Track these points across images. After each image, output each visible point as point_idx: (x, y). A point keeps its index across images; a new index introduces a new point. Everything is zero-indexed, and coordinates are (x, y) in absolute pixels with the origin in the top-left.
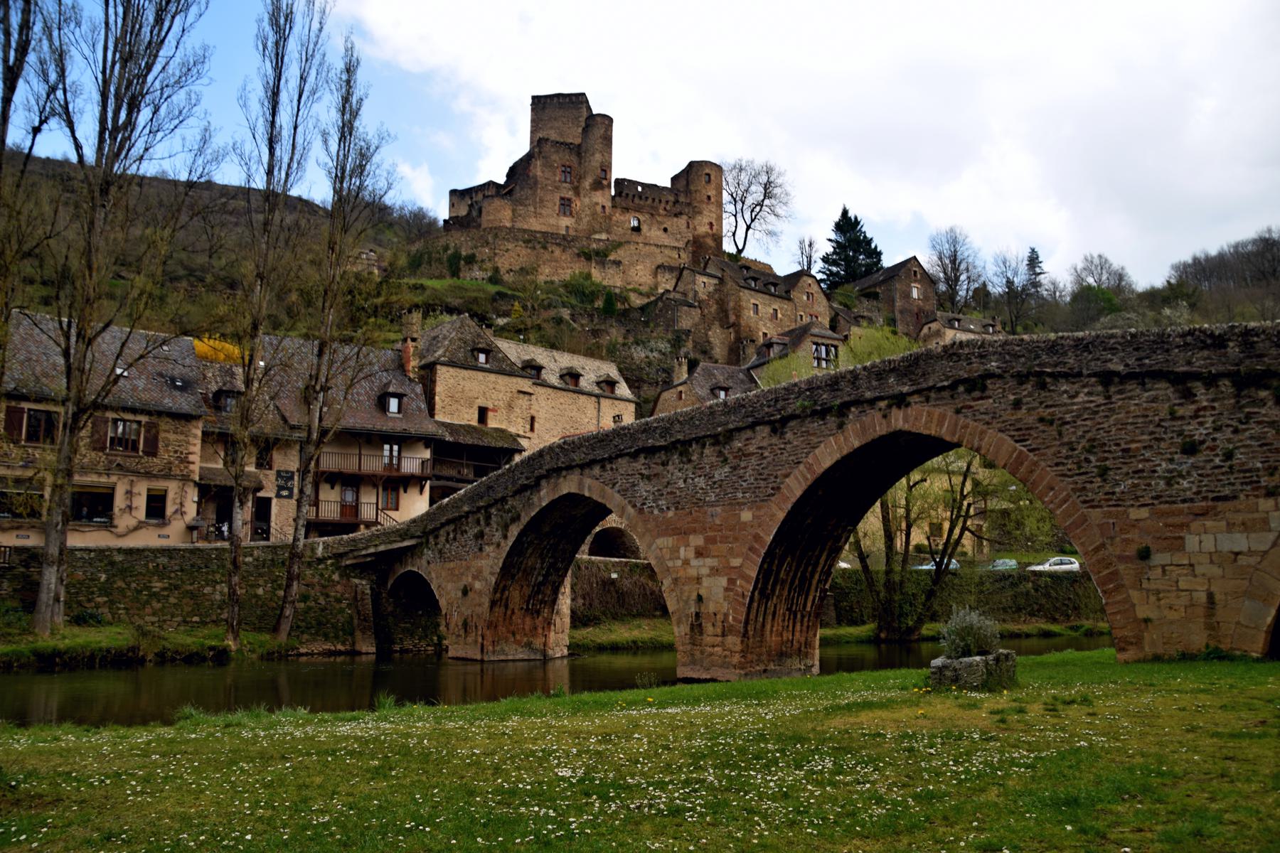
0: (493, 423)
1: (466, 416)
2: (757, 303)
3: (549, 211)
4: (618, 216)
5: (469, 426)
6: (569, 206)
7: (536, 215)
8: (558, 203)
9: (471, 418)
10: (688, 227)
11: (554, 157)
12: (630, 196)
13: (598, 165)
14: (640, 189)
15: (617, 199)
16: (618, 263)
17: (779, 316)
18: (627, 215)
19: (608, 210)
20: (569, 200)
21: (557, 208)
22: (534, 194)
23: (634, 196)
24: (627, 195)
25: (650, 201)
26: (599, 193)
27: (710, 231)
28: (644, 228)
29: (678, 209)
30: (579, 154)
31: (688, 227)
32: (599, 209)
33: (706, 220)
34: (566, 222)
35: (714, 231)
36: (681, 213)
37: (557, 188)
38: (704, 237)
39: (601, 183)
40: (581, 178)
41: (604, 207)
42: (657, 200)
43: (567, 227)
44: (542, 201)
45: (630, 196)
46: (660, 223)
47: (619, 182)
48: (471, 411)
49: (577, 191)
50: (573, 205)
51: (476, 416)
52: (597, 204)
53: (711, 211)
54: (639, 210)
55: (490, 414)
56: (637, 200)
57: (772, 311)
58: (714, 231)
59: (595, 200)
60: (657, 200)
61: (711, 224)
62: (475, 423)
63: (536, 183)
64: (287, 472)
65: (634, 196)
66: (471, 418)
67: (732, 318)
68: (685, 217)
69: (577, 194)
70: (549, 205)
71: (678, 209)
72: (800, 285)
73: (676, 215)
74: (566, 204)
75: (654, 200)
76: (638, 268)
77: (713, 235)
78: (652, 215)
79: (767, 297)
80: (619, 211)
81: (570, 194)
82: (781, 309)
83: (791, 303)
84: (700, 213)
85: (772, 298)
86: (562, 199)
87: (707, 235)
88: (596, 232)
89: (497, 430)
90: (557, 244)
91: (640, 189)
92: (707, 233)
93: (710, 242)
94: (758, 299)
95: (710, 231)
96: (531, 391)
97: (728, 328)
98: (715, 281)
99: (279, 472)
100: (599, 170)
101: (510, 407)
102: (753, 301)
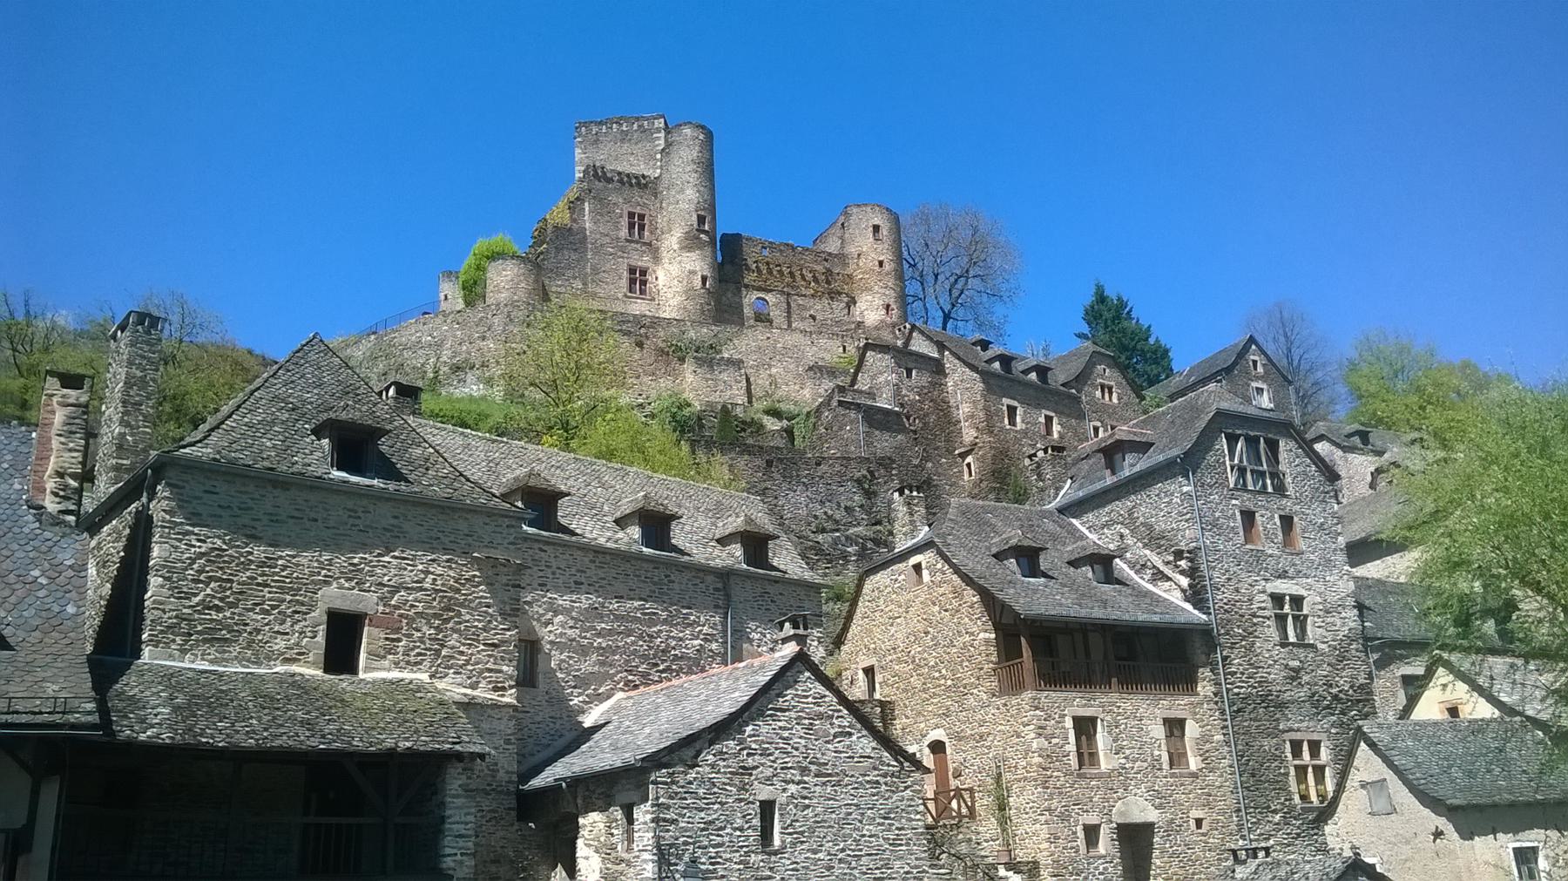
6: (644, 283)
8: (626, 274)
15: (728, 267)
21: (624, 283)
22: (582, 260)
26: (694, 255)
32: (698, 282)
33: (878, 302)
35: (894, 319)
38: (877, 328)
39: (698, 238)
41: (704, 279)
44: (596, 271)
52: (693, 272)
57: (1042, 420)
63: (585, 237)
67: (969, 434)
69: (657, 259)
74: (638, 280)
76: (774, 370)
81: (644, 261)
92: (882, 321)
100: (695, 218)
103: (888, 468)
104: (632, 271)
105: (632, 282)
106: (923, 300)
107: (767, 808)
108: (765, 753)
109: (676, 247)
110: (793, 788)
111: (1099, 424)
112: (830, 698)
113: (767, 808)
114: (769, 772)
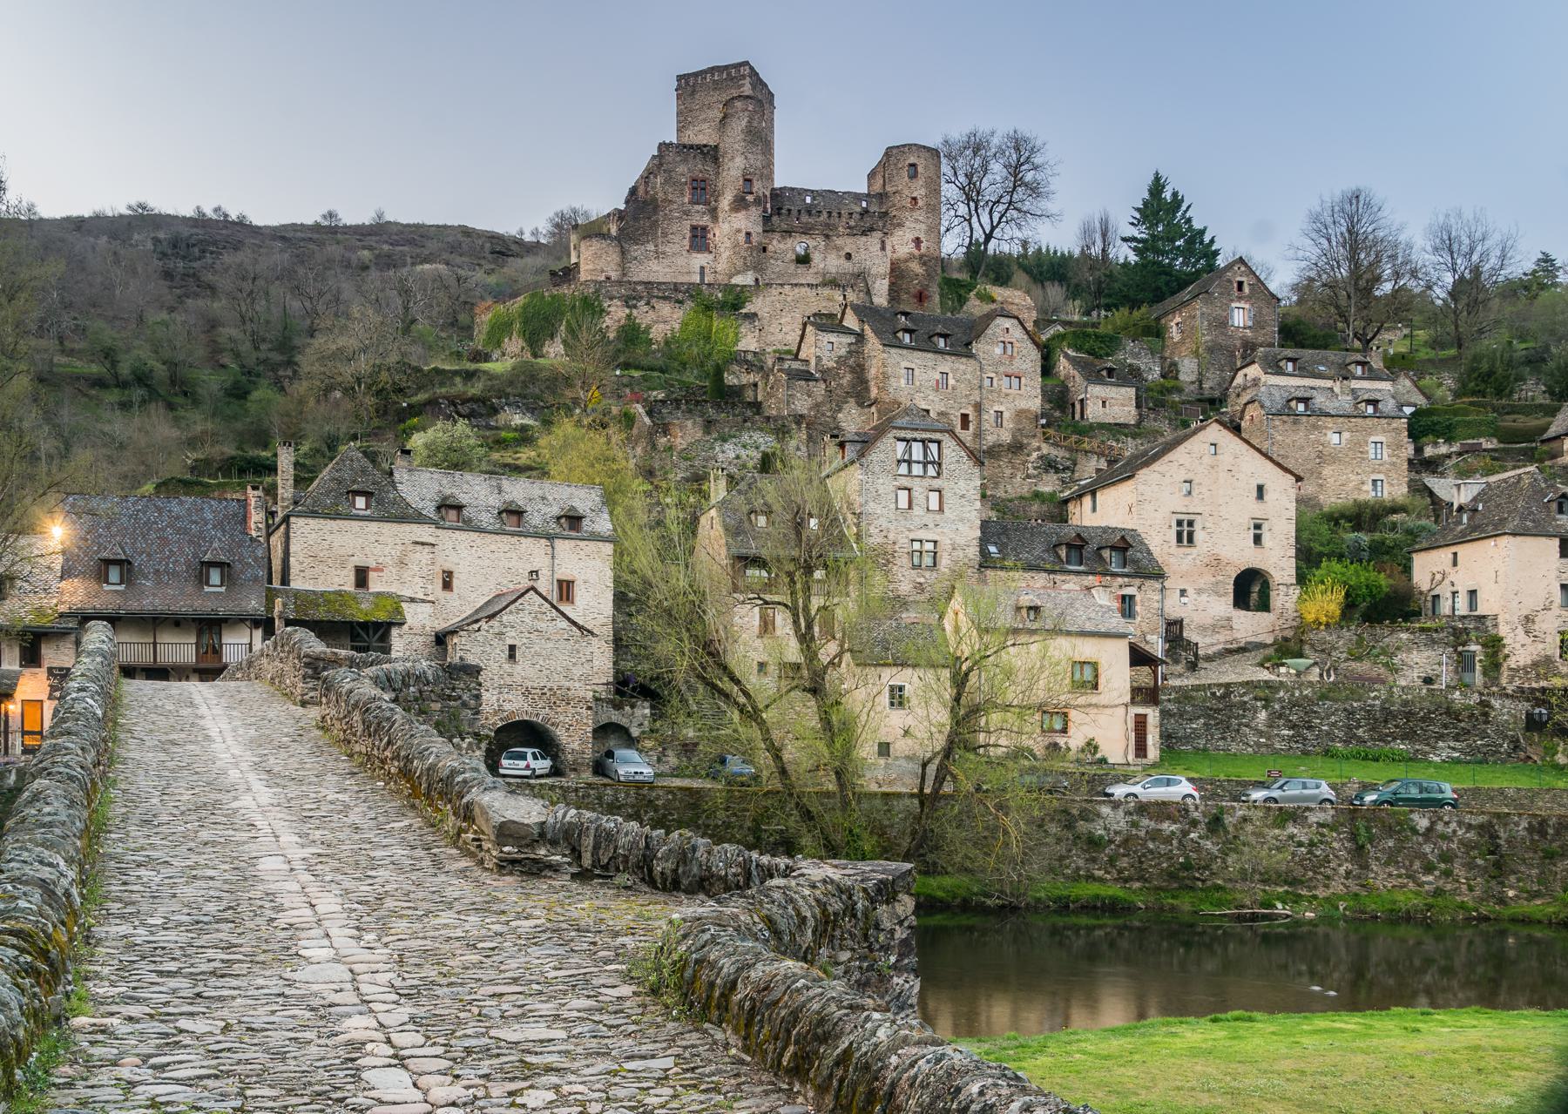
0: (376, 585)
1: (337, 579)
2: (913, 366)
3: (676, 248)
4: (776, 244)
5: (339, 593)
7: (658, 255)
8: (688, 235)
9: (344, 581)
10: (883, 248)
11: (682, 169)
12: (794, 213)
13: (739, 173)
14: (808, 200)
15: (775, 218)
16: (752, 316)
17: (951, 382)
18: (789, 241)
19: (755, 239)
20: (704, 229)
21: (686, 242)
23: (799, 211)
24: (789, 210)
25: (825, 215)
26: (741, 215)
27: (916, 252)
28: (816, 257)
29: (868, 222)
30: (716, 160)
31: (883, 248)
32: (741, 237)
33: (910, 236)
34: (700, 259)
35: (923, 250)
36: (872, 229)
37: (687, 213)
38: (906, 261)
39: (743, 199)
40: (717, 195)
41: (748, 234)
42: (835, 214)
43: (702, 268)
44: (665, 235)
45: (794, 213)
46: (838, 249)
47: (777, 195)
48: (345, 572)
49: (714, 213)
50: (710, 236)
51: (352, 578)
52: (739, 231)
53: (917, 221)
54: (806, 231)
55: (372, 575)
56: (805, 218)
57: (938, 376)
58: (923, 250)
59: (736, 226)
60: (835, 214)
61: (917, 241)
62: (349, 586)
64: (61, 669)
65: (799, 211)
66: (344, 581)
67: (874, 392)
68: (878, 234)
69: (715, 218)
70: (676, 239)
71: (868, 222)
72: (989, 331)
73: (864, 233)
75: (830, 213)
76: (783, 321)
77: (921, 257)
78: (827, 237)
79: (930, 355)
80: (777, 236)
81: (705, 220)
82: (955, 371)
83: (972, 361)
84: (900, 225)
85: (939, 357)
86: (694, 228)
87: (911, 257)
88: (738, 273)
89: (379, 594)
90: (665, 298)
91: (808, 200)
93: (916, 267)
94: (917, 359)
95: (916, 252)
96: (431, 540)
97: (870, 406)
98: (852, 339)
99: (50, 670)
101: (402, 563)
102: (905, 364)
103: (798, 423)
104: (694, 228)
105: (694, 236)
106: (969, 221)
107: (512, 648)
108: (513, 627)
109: (727, 208)
110: (525, 641)
111: (993, 375)
112: (547, 605)
113: (512, 648)
114: (513, 634)
